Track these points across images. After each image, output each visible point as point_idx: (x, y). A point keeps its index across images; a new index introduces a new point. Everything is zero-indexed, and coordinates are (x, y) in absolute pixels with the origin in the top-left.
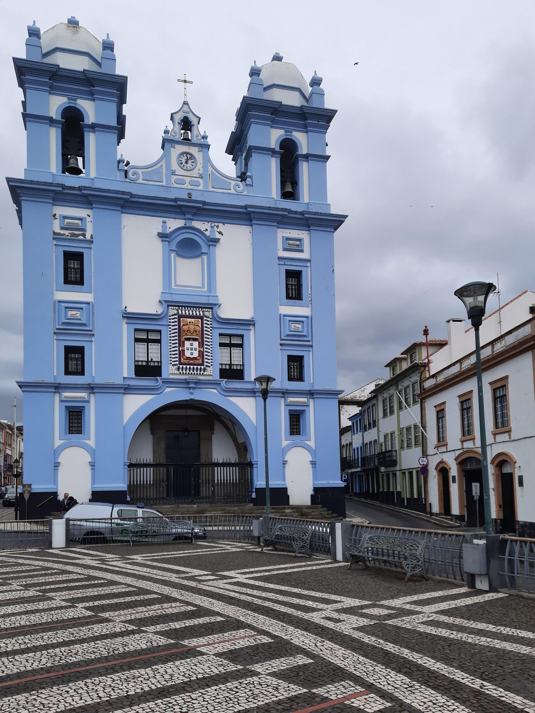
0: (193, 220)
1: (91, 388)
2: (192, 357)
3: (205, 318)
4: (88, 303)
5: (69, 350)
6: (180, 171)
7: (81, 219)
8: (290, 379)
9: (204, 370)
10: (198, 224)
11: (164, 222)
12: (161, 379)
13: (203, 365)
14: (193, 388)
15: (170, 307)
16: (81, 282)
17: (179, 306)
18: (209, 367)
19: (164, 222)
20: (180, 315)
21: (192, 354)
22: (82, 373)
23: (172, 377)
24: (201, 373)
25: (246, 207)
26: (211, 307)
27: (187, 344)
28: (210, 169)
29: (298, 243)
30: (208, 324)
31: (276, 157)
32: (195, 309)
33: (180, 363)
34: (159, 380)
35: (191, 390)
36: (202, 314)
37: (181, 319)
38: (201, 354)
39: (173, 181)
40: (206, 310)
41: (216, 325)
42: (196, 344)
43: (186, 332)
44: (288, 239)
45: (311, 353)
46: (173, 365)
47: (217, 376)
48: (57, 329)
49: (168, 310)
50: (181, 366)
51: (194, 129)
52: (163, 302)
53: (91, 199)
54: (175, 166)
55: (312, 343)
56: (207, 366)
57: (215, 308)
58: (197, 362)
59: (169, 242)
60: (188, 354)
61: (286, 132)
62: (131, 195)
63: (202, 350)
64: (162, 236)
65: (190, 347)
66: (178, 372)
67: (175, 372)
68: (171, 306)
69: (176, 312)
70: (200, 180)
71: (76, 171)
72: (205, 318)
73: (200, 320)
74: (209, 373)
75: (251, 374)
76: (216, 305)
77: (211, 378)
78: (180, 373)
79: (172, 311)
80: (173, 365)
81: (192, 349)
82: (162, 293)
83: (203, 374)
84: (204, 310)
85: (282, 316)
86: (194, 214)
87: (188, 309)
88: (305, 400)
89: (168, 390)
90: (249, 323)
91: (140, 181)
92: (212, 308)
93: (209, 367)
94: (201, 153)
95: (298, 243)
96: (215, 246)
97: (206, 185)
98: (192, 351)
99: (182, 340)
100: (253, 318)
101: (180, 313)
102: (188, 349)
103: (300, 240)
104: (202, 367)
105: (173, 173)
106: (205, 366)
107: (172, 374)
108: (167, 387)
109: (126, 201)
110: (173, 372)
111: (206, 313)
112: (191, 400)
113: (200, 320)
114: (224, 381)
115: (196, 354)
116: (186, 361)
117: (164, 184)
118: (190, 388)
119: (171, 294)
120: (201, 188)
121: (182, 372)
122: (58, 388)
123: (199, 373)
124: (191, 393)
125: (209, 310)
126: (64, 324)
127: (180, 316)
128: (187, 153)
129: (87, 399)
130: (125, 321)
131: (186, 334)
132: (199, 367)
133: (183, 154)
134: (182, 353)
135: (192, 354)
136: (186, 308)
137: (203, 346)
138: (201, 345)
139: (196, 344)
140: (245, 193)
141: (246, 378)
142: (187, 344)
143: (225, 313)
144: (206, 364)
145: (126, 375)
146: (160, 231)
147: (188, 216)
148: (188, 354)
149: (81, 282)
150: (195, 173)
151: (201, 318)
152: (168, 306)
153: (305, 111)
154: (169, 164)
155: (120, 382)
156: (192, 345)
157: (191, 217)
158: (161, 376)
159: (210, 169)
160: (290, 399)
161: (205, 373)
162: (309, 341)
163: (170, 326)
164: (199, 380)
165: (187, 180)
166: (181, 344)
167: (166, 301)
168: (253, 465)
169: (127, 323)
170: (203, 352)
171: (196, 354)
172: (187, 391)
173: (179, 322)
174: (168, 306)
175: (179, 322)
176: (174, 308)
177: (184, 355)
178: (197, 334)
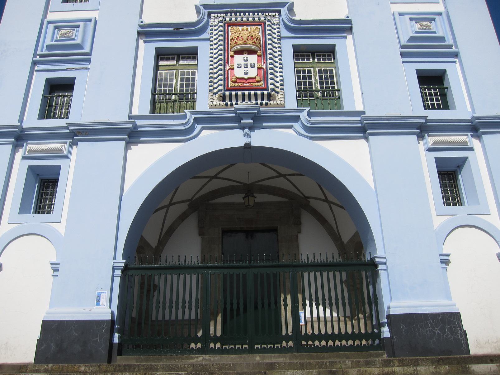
2: (246, 77)
3: (268, 23)
9: (269, 97)
12: (192, 113)
13: (266, 89)
15: (212, 15)
17: (226, 13)
18: (278, 93)
20: (227, 23)
21: (246, 74)
24: (264, 102)
32: (251, 14)
34: (188, 114)
36: (262, 19)
37: (230, 28)
40: (270, 14)
43: (236, 40)
45: (458, 65)
46: (215, 94)
49: (208, 22)
50: (227, 93)
52: (202, 8)
55: (457, 47)
56: (273, 90)
57: (284, 10)
63: (264, 67)
66: (222, 103)
67: (218, 103)
68: (214, 13)
72: (268, 23)
73: (260, 27)
74: (279, 102)
76: (283, 5)
78: (227, 105)
80: (215, 94)
81: (246, 67)
83: (266, 104)
84: (267, 14)
85: (397, 16)
87: (240, 15)
89: (205, 133)
92: (279, 12)
93: (278, 93)
98: (246, 69)
99: (231, 53)
100: (348, 17)
101: (227, 19)
102: (239, 67)
104: (265, 92)
106: (270, 91)
108: (203, 128)
110: (214, 103)
111: (269, 18)
112: (247, 146)
114: (305, 113)
116: (236, 84)
121: (229, 103)
123: (259, 102)
124: (247, 135)
125: (274, 14)
131: (236, 42)
132: (259, 92)
136: (238, 14)
137: (265, 61)
139: (253, 59)
142: (239, 59)
143: (301, 14)
144: (270, 87)
145: (135, 113)
161: (272, 102)
163: (211, 39)
167: (206, 7)
168: (376, 266)
171: (253, 73)
172: (239, 132)
173: (226, 32)
174: (209, 14)
175: (226, 32)
176: (219, 15)
178: (254, 42)
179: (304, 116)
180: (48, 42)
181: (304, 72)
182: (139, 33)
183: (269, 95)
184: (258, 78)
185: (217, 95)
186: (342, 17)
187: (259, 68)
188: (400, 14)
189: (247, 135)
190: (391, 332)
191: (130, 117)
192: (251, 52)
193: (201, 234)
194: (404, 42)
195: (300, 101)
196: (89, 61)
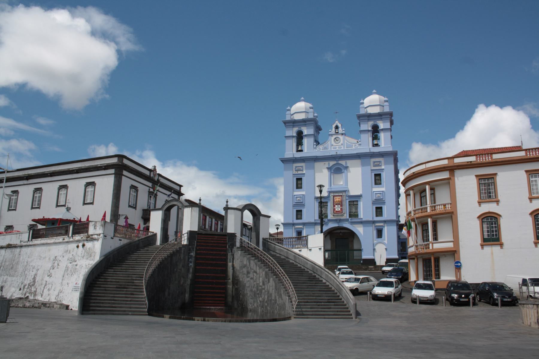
0: (339, 161)
1: (304, 224)
2: (338, 210)
4: (303, 195)
5: (297, 211)
6: (334, 144)
7: (301, 167)
8: (377, 216)
10: (340, 162)
11: (329, 163)
13: (342, 213)
14: (339, 222)
16: (301, 188)
17: (334, 192)
19: (329, 163)
21: (338, 210)
22: (301, 219)
23: (331, 218)
25: (357, 154)
26: (345, 191)
27: (336, 206)
28: (345, 141)
29: (379, 163)
30: (344, 198)
31: (370, 132)
33: (334, 213)
35: (338, 223)
38: (341, 209)
39: (332, 148)
41: (347, 198)
42: (339, 206)
44: (375, 162)
47: (348, 217)
48: (294, 205)
51: (340, 129)
53: (304, 160)
54: (333, 142)
58: (340, 212)
59: (331, 170)
60: (336, 210)
61: (374, 122)
62: (317, 157)
64: (328, 168)
65: (337, 207)
69: (332, 195)
70: (342, 146)
71: (301, 151)
73: (341, 197)
75: (361, 215)
76: (347, 190)
77: (345, 218)
79: (332, 195)
81: (338, 208)
82: (328, 188)
86: (339, 159)
88: (382, 224)
89: (330, 223)
90: (360, 196)
91: (321, 150)
94: (342, 137)
95: (379, 163)
96: (347, 169)
97: (344, 147)
99: (335, 204)
102: (337, 208)
103: (379, 162)
104: (342, 214)
105: (332, 145)
107: (331, 217)
109: (315, 158)
113: (341, 197)
115: (339, 209)
117: (329, 150)
118: (337, 222)
119: (331, 188)
120: (342, 149)
122: (294, 224)
126: (296, 203)
127: (334, 196)
128: (337, 138)
129: (303, 228)
130: (316, 199)
133: (335, 138)
134: (334, 209)
135: (338, 210)
137: (342, 206)
138: (341, 206)
139: (339, 206)
140: (359, 148)
141: (359, 217)
142: (336, 206)
144: (343, 213)
145: (316, 219)
146: (327, 167)
147: (337, 160)
148: (336, 210)
149: (301, 188)
150: (340, 144)
151: (342, 196)
152: (330, 193)
153: (380, 114)
154: (331, 142)
155: (313, 221)
156: (338, 206)
157: (338, 160)
158: (327, 218)
159: (345, 141)
160: (377, 224)
162: (384, 201)
164: (340, 219)
165: (337, 147)
166: (334, 206)
167: (329, 191)
169: (316, 200)
170: (342, 209)
171: (339, 209)
173: (334, 198)
174: (330, 193)
175: (334, 198)
177: (335, 210)
179: (350, 220)
180: (295, 201)
181: (351, 207)
182: (315, 198)
183: (343, 215)
184: (340, 211)
185: (332, 215)
186: (360, 194)
187: (341, 208)
188: (374, 192)
189: (338, 224)
190: (363, 262)
191: (315, 220)
192: (339, 204)
193: (331, 240)
194: (373, 200)
195: (349, 217)
196: (305, 206)
